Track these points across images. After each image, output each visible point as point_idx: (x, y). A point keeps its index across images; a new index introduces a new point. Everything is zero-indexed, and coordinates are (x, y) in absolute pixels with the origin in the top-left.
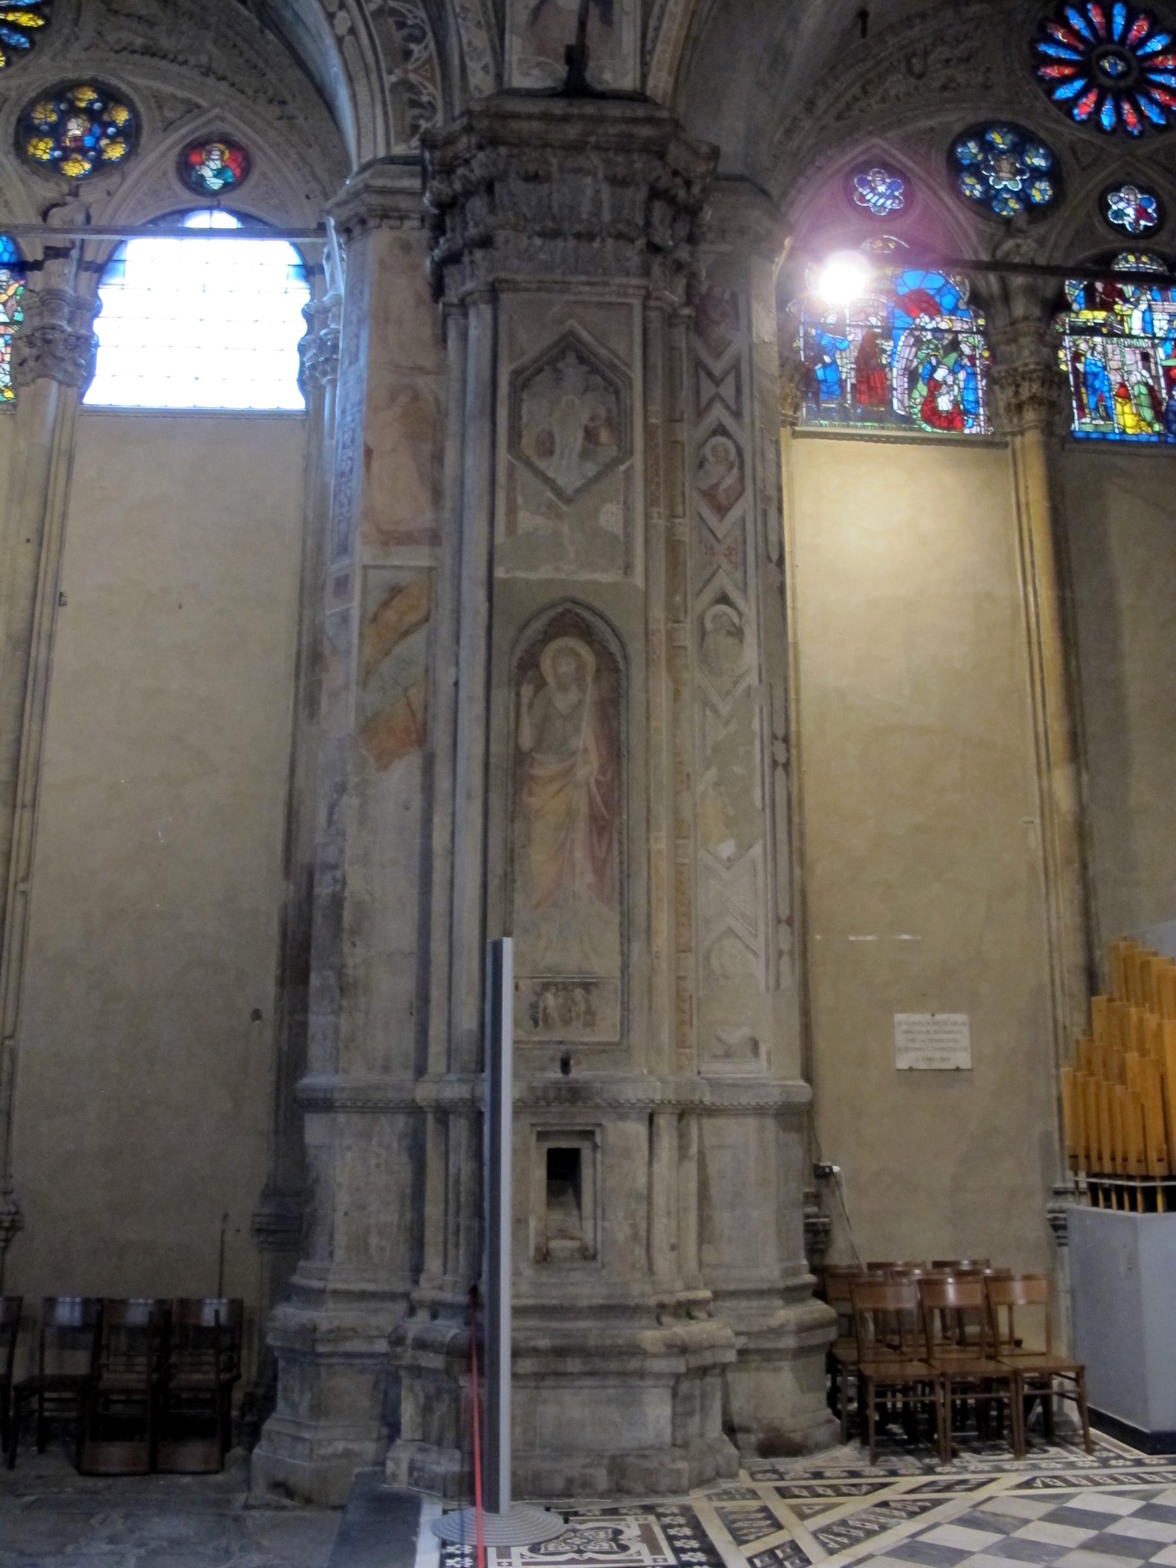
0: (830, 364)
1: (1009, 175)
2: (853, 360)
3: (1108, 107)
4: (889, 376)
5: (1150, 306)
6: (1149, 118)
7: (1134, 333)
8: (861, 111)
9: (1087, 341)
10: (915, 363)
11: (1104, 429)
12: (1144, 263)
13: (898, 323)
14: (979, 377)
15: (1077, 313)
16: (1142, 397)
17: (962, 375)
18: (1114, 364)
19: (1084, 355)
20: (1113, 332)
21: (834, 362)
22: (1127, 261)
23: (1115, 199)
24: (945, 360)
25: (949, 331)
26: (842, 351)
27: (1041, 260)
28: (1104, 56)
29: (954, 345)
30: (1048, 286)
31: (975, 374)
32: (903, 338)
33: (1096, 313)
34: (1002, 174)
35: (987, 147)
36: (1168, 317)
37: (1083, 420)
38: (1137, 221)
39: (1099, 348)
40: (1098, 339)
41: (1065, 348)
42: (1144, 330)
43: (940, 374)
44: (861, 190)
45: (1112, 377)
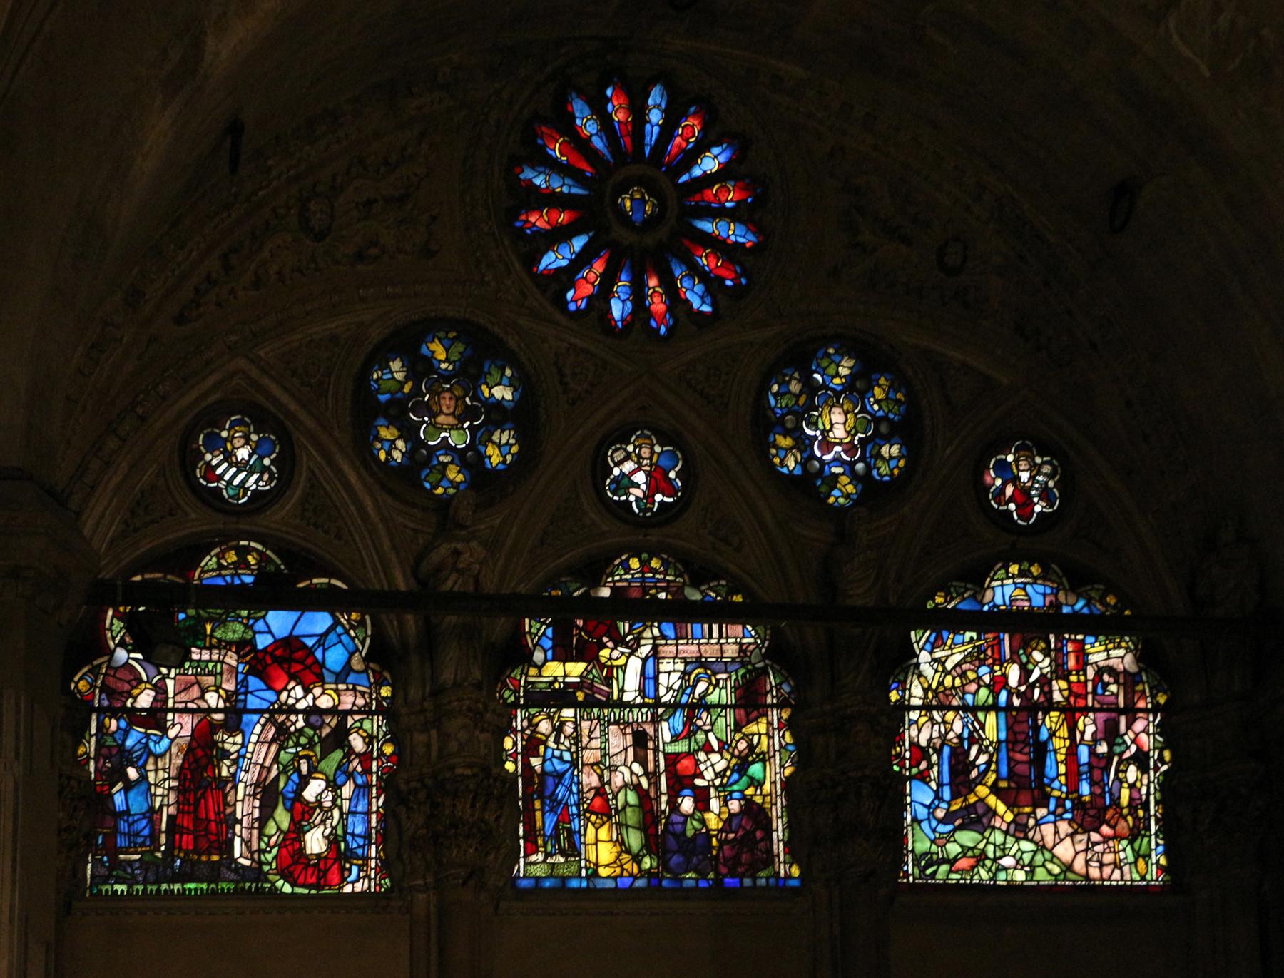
0: (137, 782)
1: (451, 420)
2: (174, 773)
3: (622, 285)
4: (230, 798)
5: (655, 648)
6: (687, 301)
7: (627, 697)
8: (219, 304)
9: (550, 718)
10: (274, 773)
11: (564, 871)
12: (655, 571)
13: (253, 702)
14: (374, 790)
15: (540, 668)
16: (628, 810)
17: (347, 791)
18: (590, 756)
19: (545, 743)
20: (594, 698)
21: (143, 777)
22: (628, 569)
23: (619, 456)
24: (323, 765)
25: (333, 711)
26: (158, 757)
27: (489, 586)
28: (623, 188)
29: (339, 738)
30: (499, 627)
31: (368, 786)
32: (258, 729)
33: (569, 666)
34: (441, 419)
35: (421, 368)
36: (681, 667)
37: (533, 858)
38: (649, 496)
39: (569, 729)
40: (568, 713)
41: (515, 731)
42: (642, 691)
43: (314, 789)
44: (208, 457)
45: (585, 779)
